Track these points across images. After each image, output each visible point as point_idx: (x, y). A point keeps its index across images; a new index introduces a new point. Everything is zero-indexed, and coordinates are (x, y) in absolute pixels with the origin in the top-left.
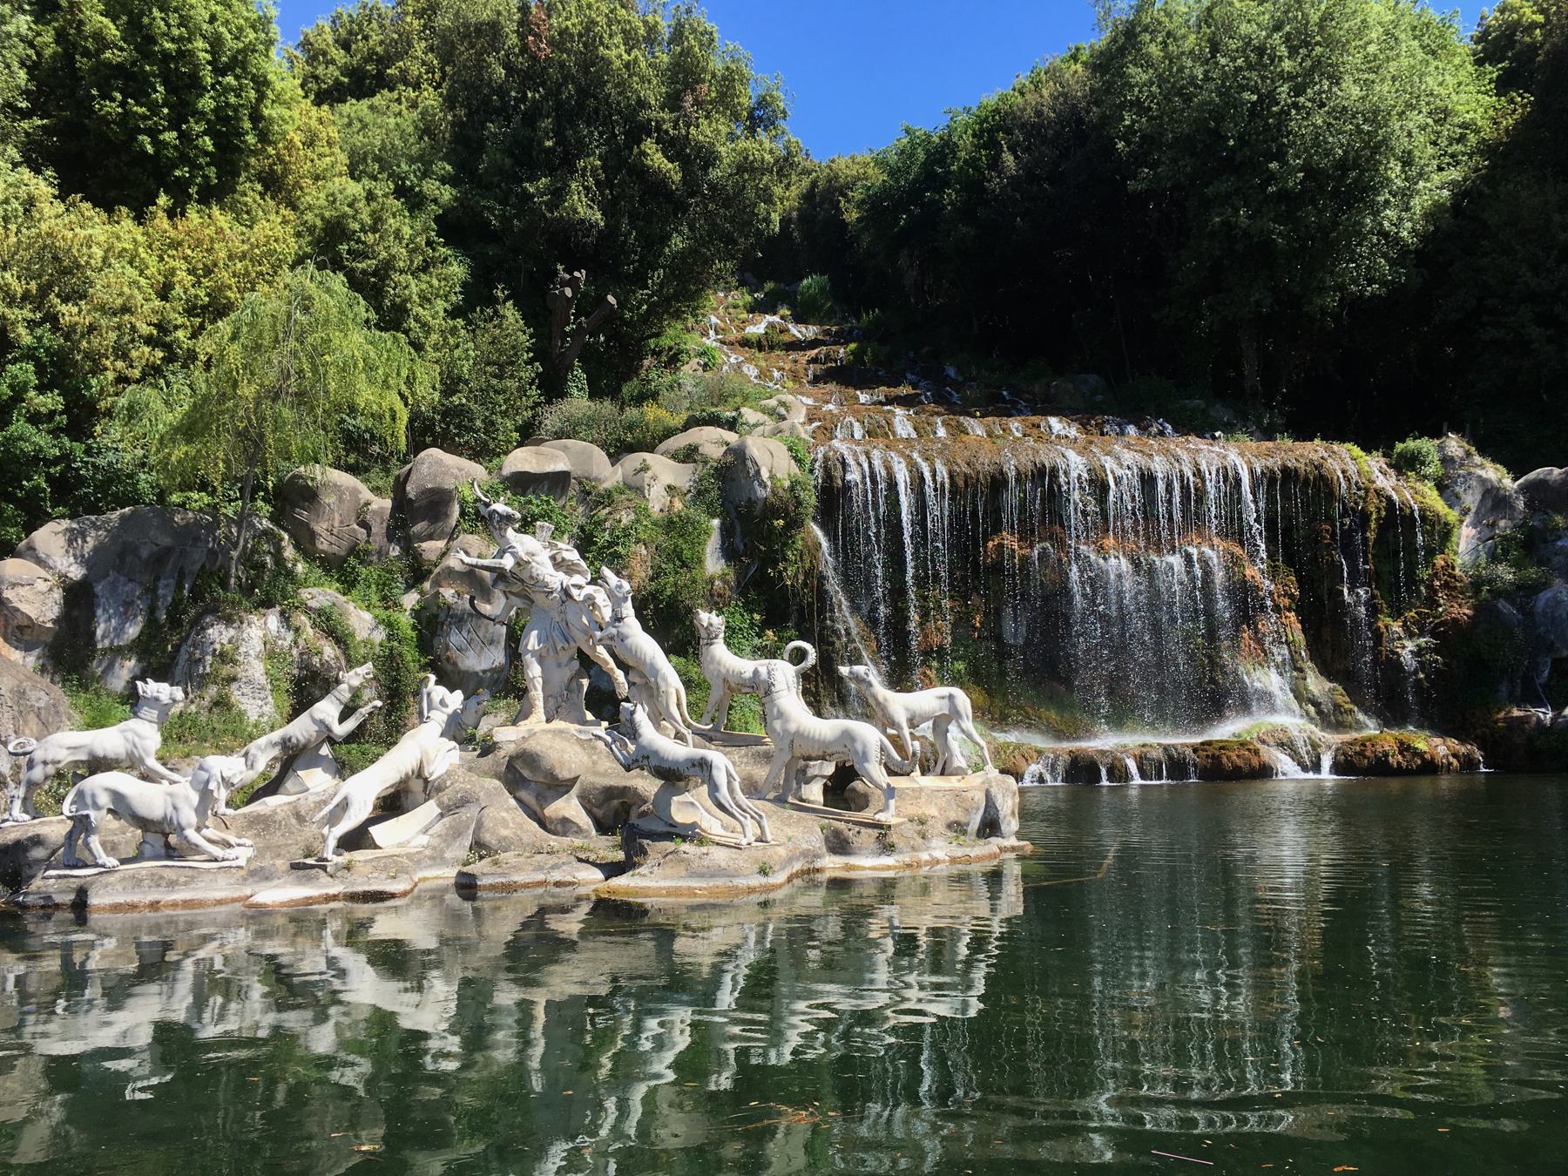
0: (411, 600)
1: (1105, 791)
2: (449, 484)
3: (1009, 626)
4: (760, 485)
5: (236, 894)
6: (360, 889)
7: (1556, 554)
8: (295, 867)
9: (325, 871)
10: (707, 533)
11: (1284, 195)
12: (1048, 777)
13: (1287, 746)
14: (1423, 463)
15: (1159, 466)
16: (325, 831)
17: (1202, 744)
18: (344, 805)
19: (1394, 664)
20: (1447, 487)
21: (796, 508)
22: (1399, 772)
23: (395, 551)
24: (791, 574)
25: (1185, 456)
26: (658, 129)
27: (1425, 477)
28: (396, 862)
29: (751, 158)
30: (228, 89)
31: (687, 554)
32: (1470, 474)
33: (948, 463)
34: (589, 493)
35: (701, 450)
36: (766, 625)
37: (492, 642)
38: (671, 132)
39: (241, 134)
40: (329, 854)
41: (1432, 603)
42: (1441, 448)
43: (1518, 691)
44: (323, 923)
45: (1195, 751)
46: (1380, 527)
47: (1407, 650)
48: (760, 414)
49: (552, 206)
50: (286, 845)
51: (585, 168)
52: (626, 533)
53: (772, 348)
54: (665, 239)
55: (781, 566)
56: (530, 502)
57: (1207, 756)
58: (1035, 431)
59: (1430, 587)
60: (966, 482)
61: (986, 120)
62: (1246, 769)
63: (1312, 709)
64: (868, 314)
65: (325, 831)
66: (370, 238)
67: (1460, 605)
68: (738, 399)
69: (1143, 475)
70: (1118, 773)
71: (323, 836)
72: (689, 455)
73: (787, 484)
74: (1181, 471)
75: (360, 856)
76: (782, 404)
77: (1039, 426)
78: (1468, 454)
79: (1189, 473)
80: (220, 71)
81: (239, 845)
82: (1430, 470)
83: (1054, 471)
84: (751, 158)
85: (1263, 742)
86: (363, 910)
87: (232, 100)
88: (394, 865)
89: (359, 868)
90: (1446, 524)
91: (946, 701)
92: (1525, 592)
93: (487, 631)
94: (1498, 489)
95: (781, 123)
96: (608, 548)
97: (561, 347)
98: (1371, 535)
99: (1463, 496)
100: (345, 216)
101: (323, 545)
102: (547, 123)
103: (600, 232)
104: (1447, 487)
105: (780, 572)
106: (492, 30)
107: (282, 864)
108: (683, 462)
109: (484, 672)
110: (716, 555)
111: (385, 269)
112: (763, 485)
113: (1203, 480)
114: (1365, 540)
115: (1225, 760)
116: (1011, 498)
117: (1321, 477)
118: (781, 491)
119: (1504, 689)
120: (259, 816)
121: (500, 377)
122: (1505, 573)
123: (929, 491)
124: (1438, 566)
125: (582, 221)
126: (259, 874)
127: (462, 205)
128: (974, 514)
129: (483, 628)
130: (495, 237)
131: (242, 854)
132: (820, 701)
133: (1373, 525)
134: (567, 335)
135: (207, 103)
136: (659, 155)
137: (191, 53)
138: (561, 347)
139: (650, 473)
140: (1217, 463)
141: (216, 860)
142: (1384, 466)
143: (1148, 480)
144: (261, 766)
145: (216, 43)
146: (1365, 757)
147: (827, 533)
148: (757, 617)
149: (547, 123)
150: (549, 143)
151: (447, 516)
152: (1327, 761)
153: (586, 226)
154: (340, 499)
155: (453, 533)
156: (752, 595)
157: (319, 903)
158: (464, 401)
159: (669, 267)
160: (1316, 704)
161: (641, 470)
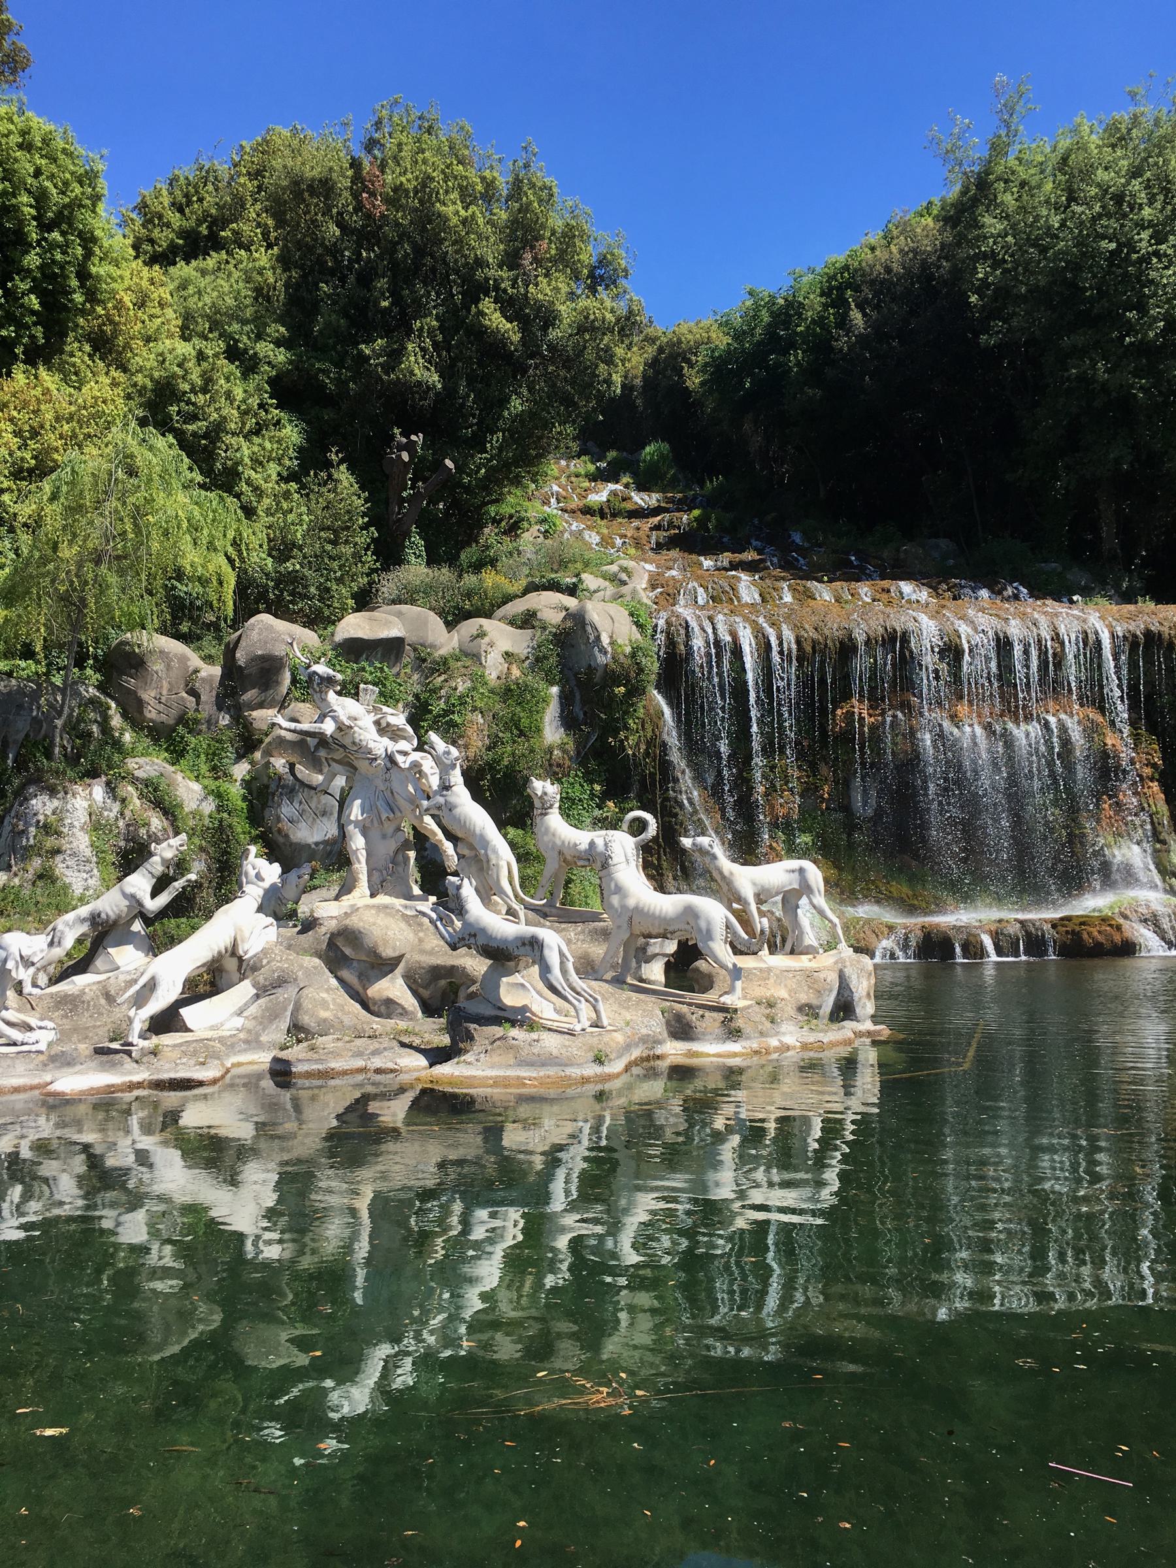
0: (241, 770)
1: (959, 969)
2: (279, 650)
3: (858, 799)
4: (600, 651)
5: (36, 1081)
6: (166, 1076)
8: (100, 1051)
9: (130, 1056)
11: (1144, 349)
12: (899, 953)
15: (1015, 630)
16: (132, 1013)
17: (1062, 919)
18: (151, 986)
21: (638, 674)
23: (225, 720)
24: (632, 743)
25: (1043, 621)
26: (497, 288)
28: (206, 1047)
29: (592, 317)
30: (53, 245)
31: (525, 722)
33: (795, 627)
34: (424, 660)
36: (606, 795)
37: (324, 814)
39: (68, 292)
40: (134, 1038)
44: (128, 1112)
45: (1054, 926)
48: (601, 580)
49: (389, 368)
50: (94, 1027)
51: (421, 329)
53: (614, 515)
54: (504, 402)
55: (622, 735)
56: (363, 669)
57: (1067, 932)
58: (885, 596)
60: (813, 648)
61: (834, 277)
62: (1108, 945)
64: (711, 481)
65: (132, 1013)
66: (201, 399)
68: (579, 566)
69: (998, 640)
70: (973, 949)
71: (129, 1018)
72: (527, 621)
73: (628, 650)
74: (1039, 635)
75: (168, 1039)
76: (624, 569)
77: (889, 591)
79: (1046, 634)
80: (45, 226)
81: (40, 1028)
83: (905, 638)
84: (592, 317)
85: (1126, 917)
86: (171, 1099)
87: (59, 257)
88: (205, 1051)
89: (167, 1053)
91: (797, 874)
93: (319, 802)
95: (623, 282)
97: (399, 513)
100: (174, 376)
101: (151, 713)
102: (382, 283)
103: (437, 394)
105: (622, 741)
106: (324, 187)
107: (85, 1048)
108: (521, 628)
109: (317, 844)
111: (216, 431)
112: (603, 651)
113: (1062, 644)
115: (1085, 936)
116: (861, 664)
118: (621, 657)
120: (66, 996)
121: (334, 543)
123: (776, 657)
125: (419, 383)
126: (60, 1060)
127: (297, 368)
128: (823, 681)
129: (315, 799)
131: (43, 1038)
132: (662, 875)
134: (403, 500)
135: (32, 260)
136: (498, 314)
137: (16, 208)
138: (399, 513)
139: (486, 640)
140: (1076, 626)
141: (15, 1044)
143: (1003, 645)
144: (69, 942)
145: (41, 198)
147: (670, 704)
148: (597, 787)
149: (382, 283)
150: (385, 304)
151: (278, 683)
153: (423, 388)
154: (168, 667)
155: (284, 701)
156: (592, 765)
157: (122, 1091)
159: (508, 430)
161: (478, 636)
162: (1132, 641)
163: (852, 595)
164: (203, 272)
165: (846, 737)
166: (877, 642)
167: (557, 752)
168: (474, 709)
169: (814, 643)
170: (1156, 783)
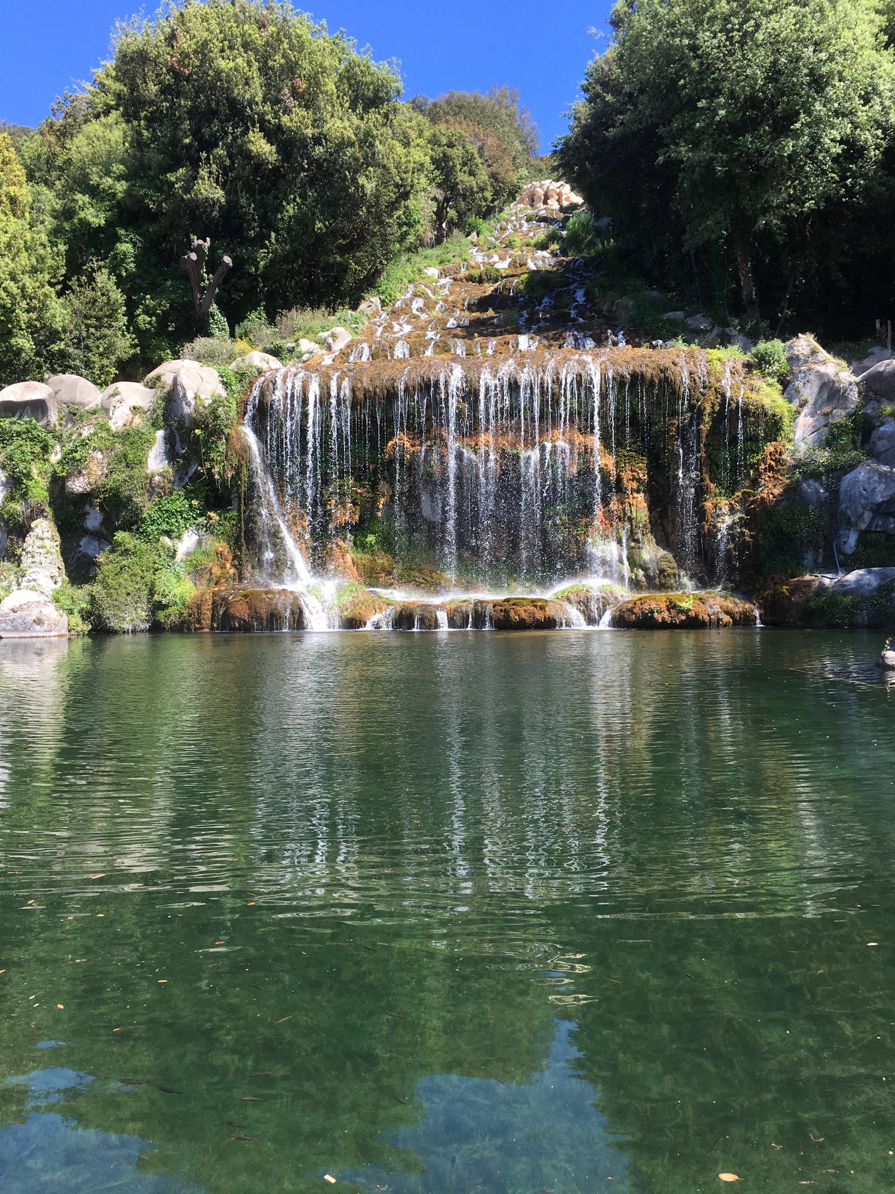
4: (186, 404)
7: (880, 438)
10: (150, 442)
13: (584, 604)
14: (768, 363)
15: (524, 378)
19: (712, 533)
20: (789, 382)
22: (664, 626)
27: (769, 374)
31: (131, 457)
32: (809, 370)
34: (75, 414)
35: (163, 378)
38: (272, 121)
41: (755, 483)
42: (791, 347)
43: (820, 559)
45: (494, 606)
46: (714, 420)
47: (725, 522)
48: (313, 343)
49: (187, 189)
52: (84, 444)
53: (489, 280)
54: (280, 209)
55: (208, 465)
56: (14, 423)
57: (501, 611)
59: (757, 470)
60: (365, 395)
62: (528, 620)
63: (641, 573)
67: (775, 486)
68: (301, 333)
69: (510, 384)
70: (429, 623)
73: (207, 403)
74: (542, 379)
76: (333, 336)
78: (814, 352)
79: (548, 379)
82: (775, 367)
83: (437, 383)
90: (774, 415)
92: (836, 471)
94: (834, 382)
96: (69, 454)
97: (201, 299)
98: (705, 428)
99: (802, 389)
103: (221, 207)
104: (789, 382)
108: (151, 388)
110: (160, 458)
114: (699, 431)
115: (512, 614)
116: (400, 407)
117: (666, 378)
118: (201, 408)
119: (809, 557)
122: (824, 457)
123: (333, 401)
124: (767, 452)
130: (154, 217)
133: (707, 419)
134: (204, 288)
136: (263, 142)
138: (201, 299)
139: (118, 398)
140: (577, 369)
142: (739, 367)
143: (514, 387)
146: (633, 613)
148: (195, 502)
149: (186, 125)
150: (187, 141)
152: (607, 617)
153: (210, 204)
158: (62, 346)
160: (645, 569)
161: (112, 395)
162: (620, 382)
163: (482, 348)
164: (105, 125)
165: (392, 461)
166: (414, 389)
167: (157, 478)
168: (95, 449)
169: (366, 391)
170: (642, 494)
